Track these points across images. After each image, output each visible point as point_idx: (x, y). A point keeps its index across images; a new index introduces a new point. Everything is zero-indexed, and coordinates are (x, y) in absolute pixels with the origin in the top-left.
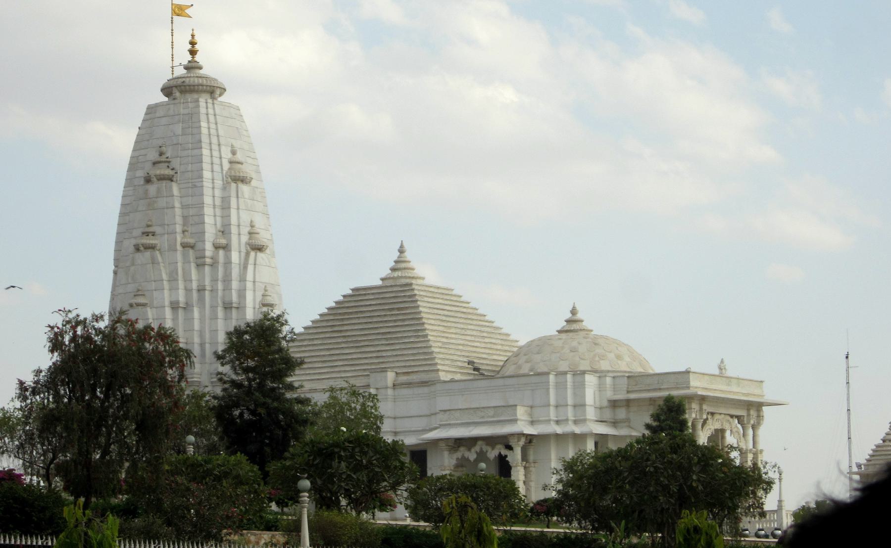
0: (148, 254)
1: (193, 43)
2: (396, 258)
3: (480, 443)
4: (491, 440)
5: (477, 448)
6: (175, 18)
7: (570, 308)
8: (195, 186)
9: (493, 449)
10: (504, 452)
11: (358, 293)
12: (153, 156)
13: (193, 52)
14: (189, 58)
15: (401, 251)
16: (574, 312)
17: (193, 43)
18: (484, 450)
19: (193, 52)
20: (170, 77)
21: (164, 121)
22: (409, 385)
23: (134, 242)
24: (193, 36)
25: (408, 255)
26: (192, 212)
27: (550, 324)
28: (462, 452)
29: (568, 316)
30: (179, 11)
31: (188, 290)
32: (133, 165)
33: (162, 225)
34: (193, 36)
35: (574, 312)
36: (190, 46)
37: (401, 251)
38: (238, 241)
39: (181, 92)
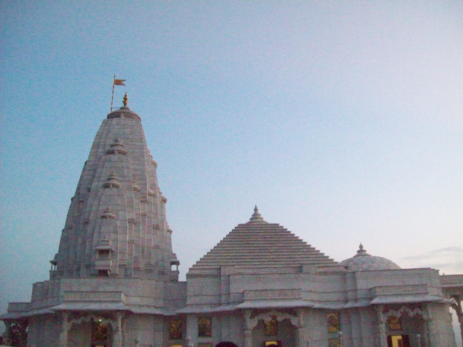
0: (115, 190)
1: (125, 99)
2: (253, 214)
3: (403, 307)
4: (412, 305)
5: (402, 310)
6: (115, 86)
7: (359, 245)
8: (139, 160)
9: (412, 311)
10: (420, 312)
11: (241, 226)
12: (111, 142)
13: (125, 104)
14: (122, 105)
15: (256, 210)
16: (361, 247)
17: (125, 99)
18: (407, 311)
19: (125, 104)
20: (109, 112)
21: (118, 127)
22: (326, 273)
23: (101, 183)
24: (126, 96)
25: (259, 212)
26: (138, 173)
27: (352, 253)
28: (391, 313)
29: (359, 249)
30: (118, 82)
31: (136, 214)
32: (96, 146)
33: (123, 176)
34: (126, 96)
35: (361, 247)
36: (123, 100)
37: (256, 210)
38: (158, 194)
39: (125, 116)
